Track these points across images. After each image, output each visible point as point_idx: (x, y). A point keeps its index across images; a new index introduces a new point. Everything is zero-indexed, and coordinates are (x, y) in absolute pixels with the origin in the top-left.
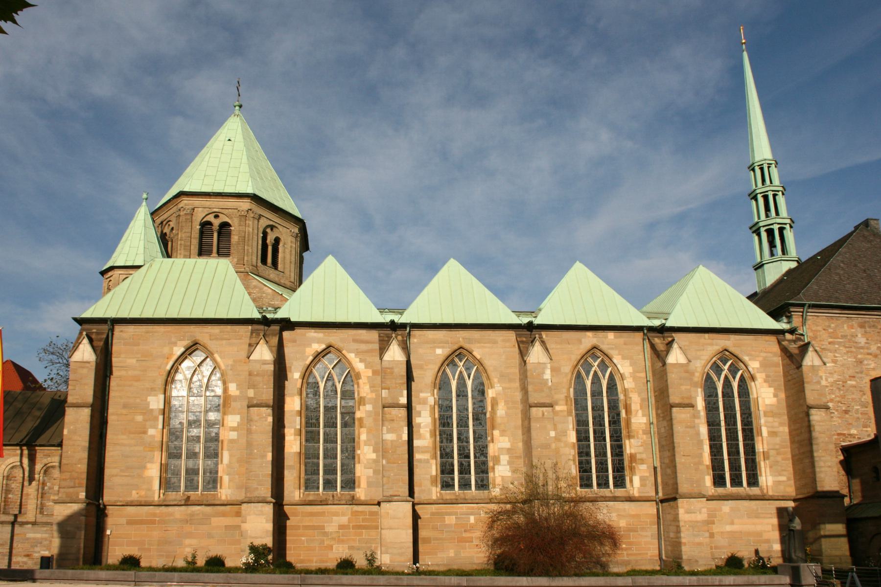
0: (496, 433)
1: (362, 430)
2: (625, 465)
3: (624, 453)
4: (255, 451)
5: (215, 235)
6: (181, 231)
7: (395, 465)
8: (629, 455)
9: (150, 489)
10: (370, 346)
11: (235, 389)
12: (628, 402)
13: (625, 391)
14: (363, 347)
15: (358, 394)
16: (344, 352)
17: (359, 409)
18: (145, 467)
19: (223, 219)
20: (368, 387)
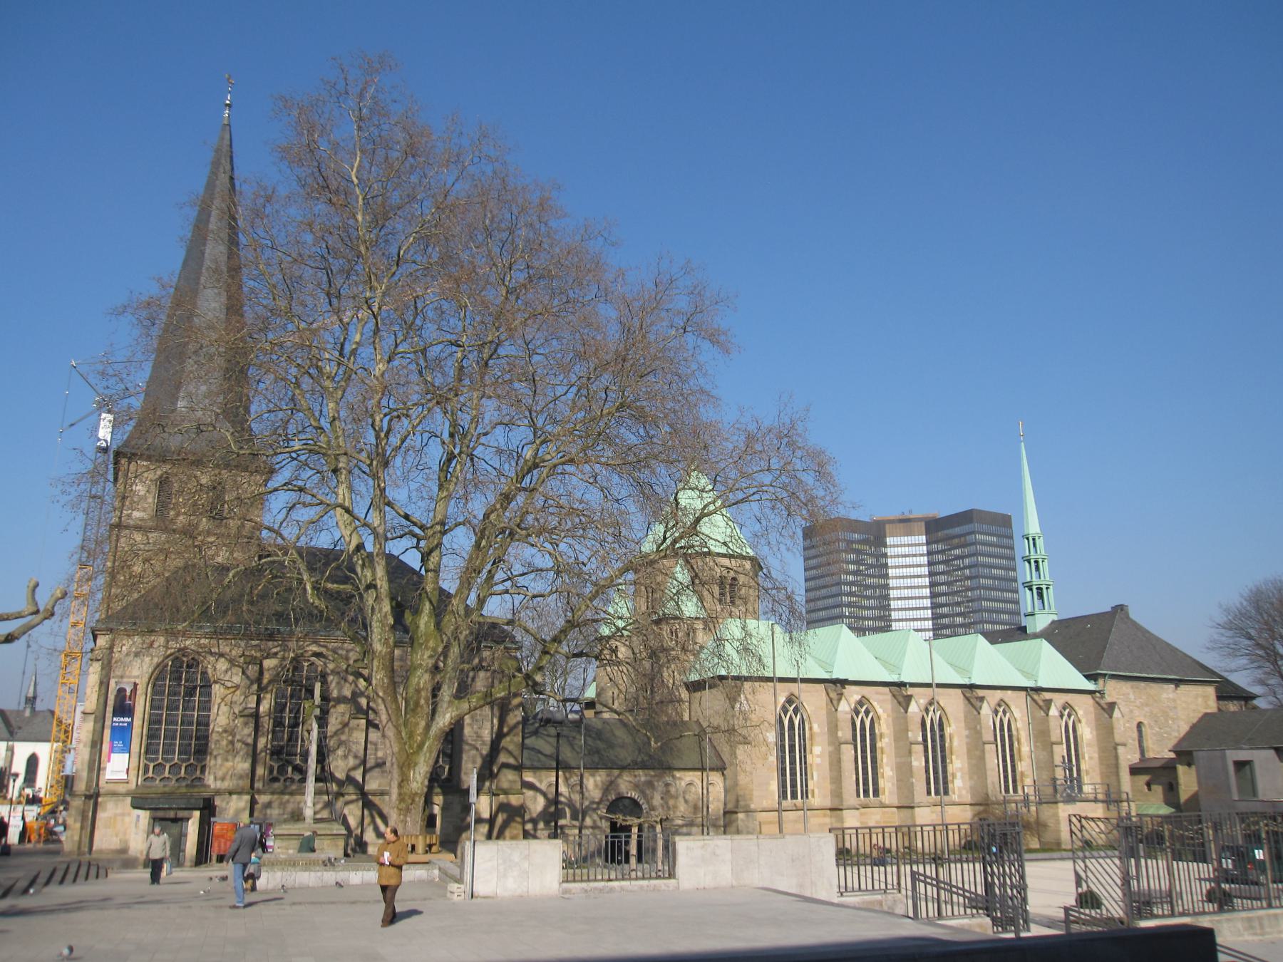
10: (885, 697)
14: (881, 697)
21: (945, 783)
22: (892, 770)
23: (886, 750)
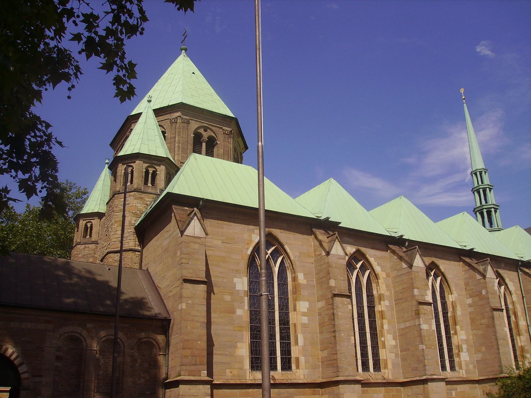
0: (458, 327)
1: (384, 321)
2: (518, 354)
3: (516, 346)
4: (343, 334)
5: (204, 145)
6: (179, 135)
7: (430, 350)
8: (520, 347)
9: (241, 369)
11: (303, 278)
12: (516, 310)
13: (513, 303)
15: (377, 291)
16: (367, 256)
17: (380, 304)
18: (236, 347)
19: (210, 133)
20: (385, 286)
21: (451, 356)
22: (394, 338)
23: (387, 314)
